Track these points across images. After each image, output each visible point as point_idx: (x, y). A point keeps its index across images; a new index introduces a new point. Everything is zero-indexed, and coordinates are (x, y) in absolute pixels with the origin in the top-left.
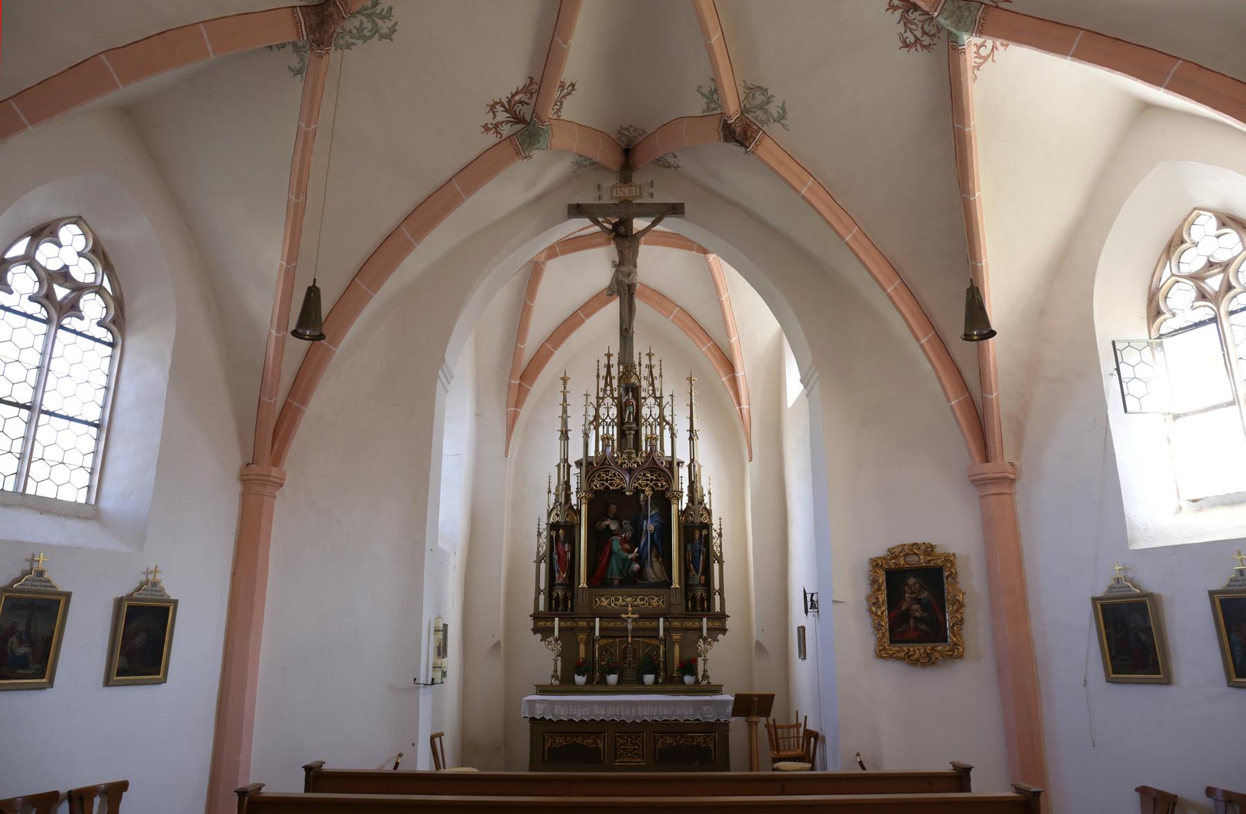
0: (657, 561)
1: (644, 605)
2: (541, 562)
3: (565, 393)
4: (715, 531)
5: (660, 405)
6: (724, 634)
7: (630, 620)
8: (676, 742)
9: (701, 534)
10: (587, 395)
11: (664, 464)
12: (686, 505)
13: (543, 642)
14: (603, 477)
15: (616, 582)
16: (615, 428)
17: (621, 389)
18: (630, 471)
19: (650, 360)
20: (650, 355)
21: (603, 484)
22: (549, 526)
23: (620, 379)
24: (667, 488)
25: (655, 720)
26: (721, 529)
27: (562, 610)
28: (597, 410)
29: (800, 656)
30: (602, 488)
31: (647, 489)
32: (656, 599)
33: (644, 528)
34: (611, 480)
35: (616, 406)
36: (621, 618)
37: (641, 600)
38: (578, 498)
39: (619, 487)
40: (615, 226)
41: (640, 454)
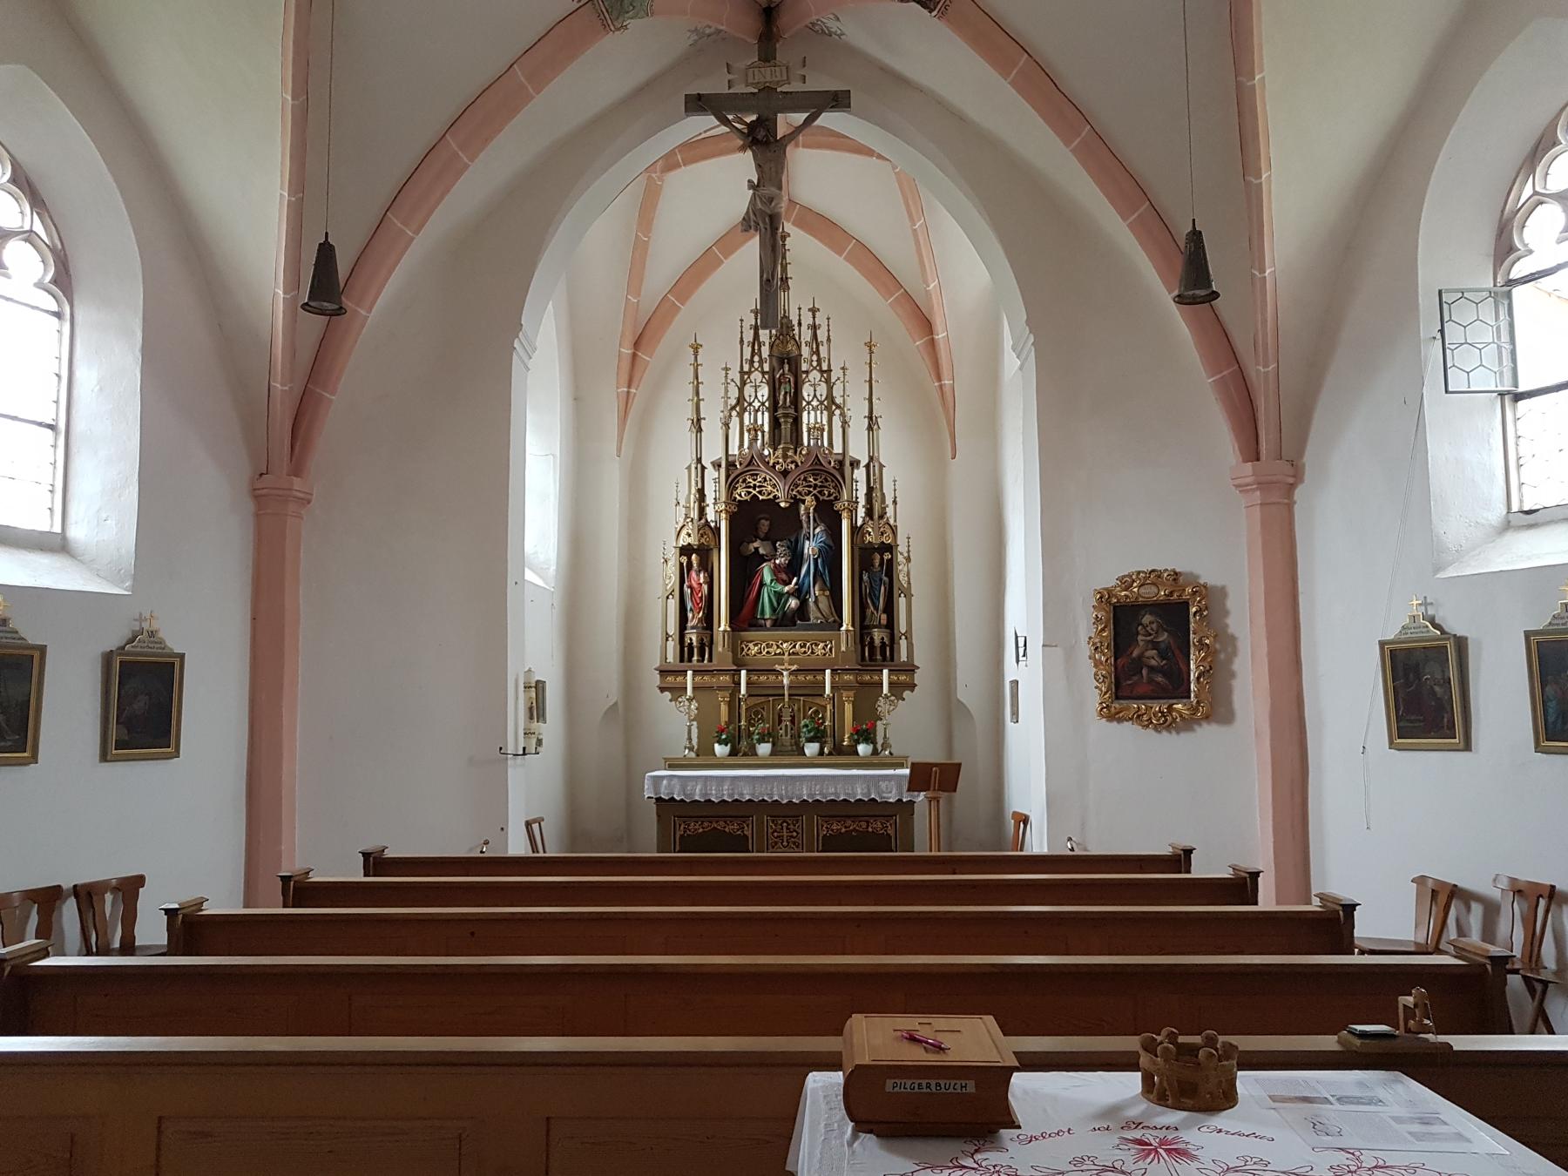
0: (824, 594)
1: (805, 652)
2: (668, 598)
3: (696, 366)
4: (901, 554)
5: (828, 381)
6: (912, 691)
7: (785, 673)
8: (846, 827)
9: (882, 559)
10: (727, 369)
11: (833, 463)
13: (673, 703)
14: (750, 482)
15: (768, 624)
16: (766, 414)
17: (774, 359)
18: (785, 473)
19: (814, 318)
20: (814, 311)
23: (771, 347)
24: (836, 497)
25: (818, 800)
26: (909, 552)
27: (698, 661)
28: (741, 390)
29: (1012, 719)
30: (748, 498)
31: (808, 498)
32: (822, 645)
33: (806, 551)
34: (760, 487)
35: (768, 384)
36: (775, 670)
37: (801, 647)
39: (771, 497)
40: (751, 126)
41: (799, 450)
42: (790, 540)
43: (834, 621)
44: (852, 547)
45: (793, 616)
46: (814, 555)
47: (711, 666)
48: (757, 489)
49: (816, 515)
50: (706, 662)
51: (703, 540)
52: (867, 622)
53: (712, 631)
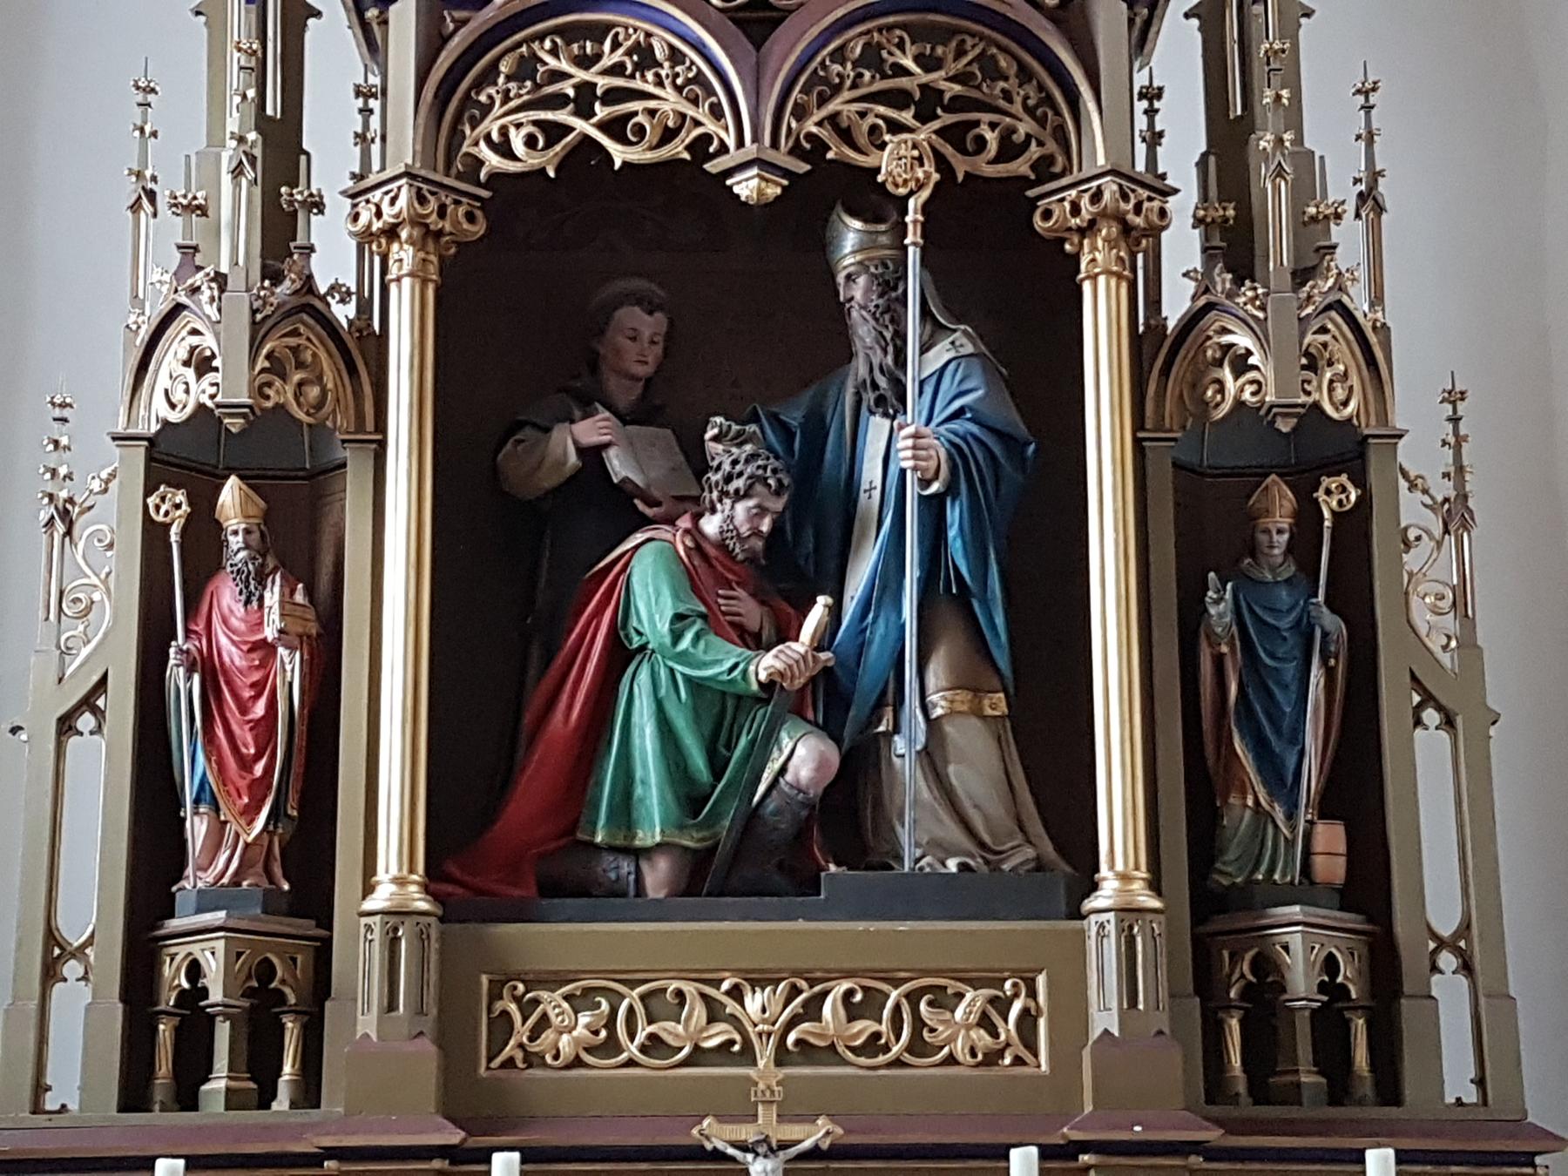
1: (874, 1045)
2: (66, 725)
12: (1190, 286)
15: (657, 876)
21: (555, 132)
22: (139, 453)
30: (547, 160)
32: (973, 1001)
33: (871, 472)
34: (612, 96)
37: (853, 1012)
38: (365, 238)
39: (678, 149)
42: (775, 419)
43: (1040, 865)
44: (1137, 442)
45: (801, 835)
46: (925, 483)
47: (312, 1126)
48: (601, 112)
49: (928, 277)
50: (281, 1103)
51: (282, 393)
52: (1229, 872)
53: (325, 919)
